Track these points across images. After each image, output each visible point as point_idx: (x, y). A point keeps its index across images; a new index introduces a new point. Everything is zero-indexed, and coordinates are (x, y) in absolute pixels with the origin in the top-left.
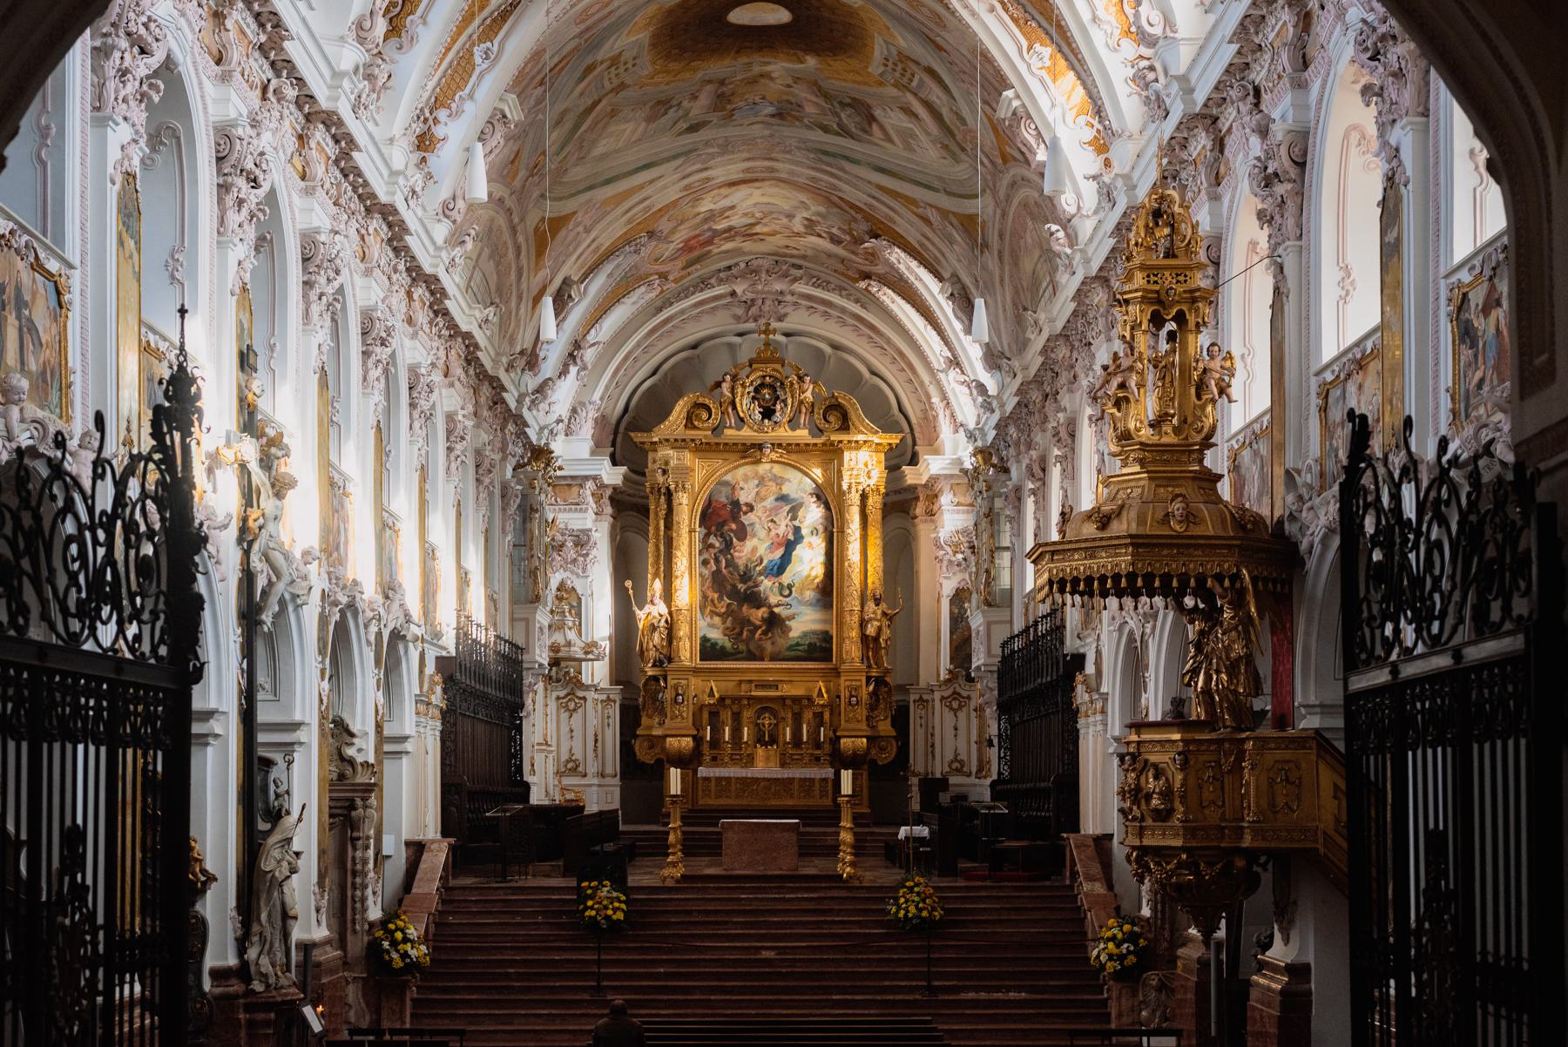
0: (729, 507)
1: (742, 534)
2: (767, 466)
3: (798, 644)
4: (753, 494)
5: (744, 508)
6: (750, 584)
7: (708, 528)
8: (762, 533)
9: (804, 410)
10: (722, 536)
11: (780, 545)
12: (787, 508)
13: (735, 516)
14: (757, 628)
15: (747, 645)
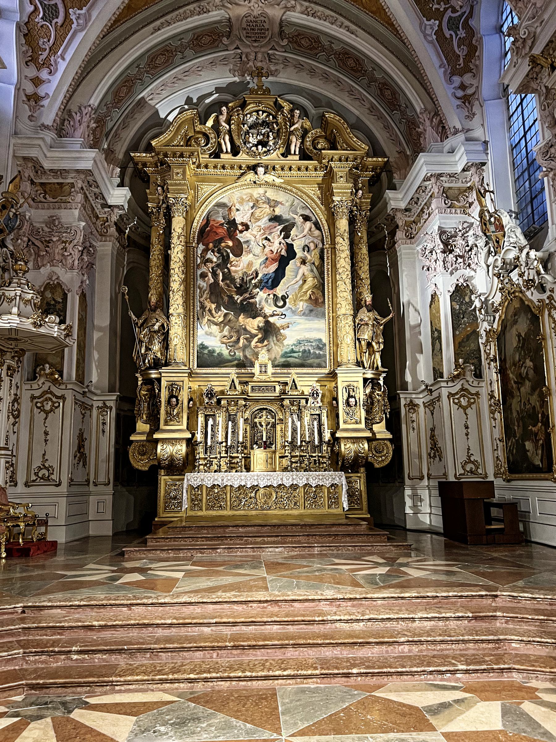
0: (226, 226)
1: (238, 250)
2: (261, 190)
3: (293, 351)
4: (249, 214)
5: (240, 227)
6: (247, 295)
7: (207, 245)
8: (257, 250)
9: (294, 140)
10: (219, 251)
11: (274, 260)
12: (280, 227)
13: (232, 236)
14: (253, 336)
15: (244, 351)
